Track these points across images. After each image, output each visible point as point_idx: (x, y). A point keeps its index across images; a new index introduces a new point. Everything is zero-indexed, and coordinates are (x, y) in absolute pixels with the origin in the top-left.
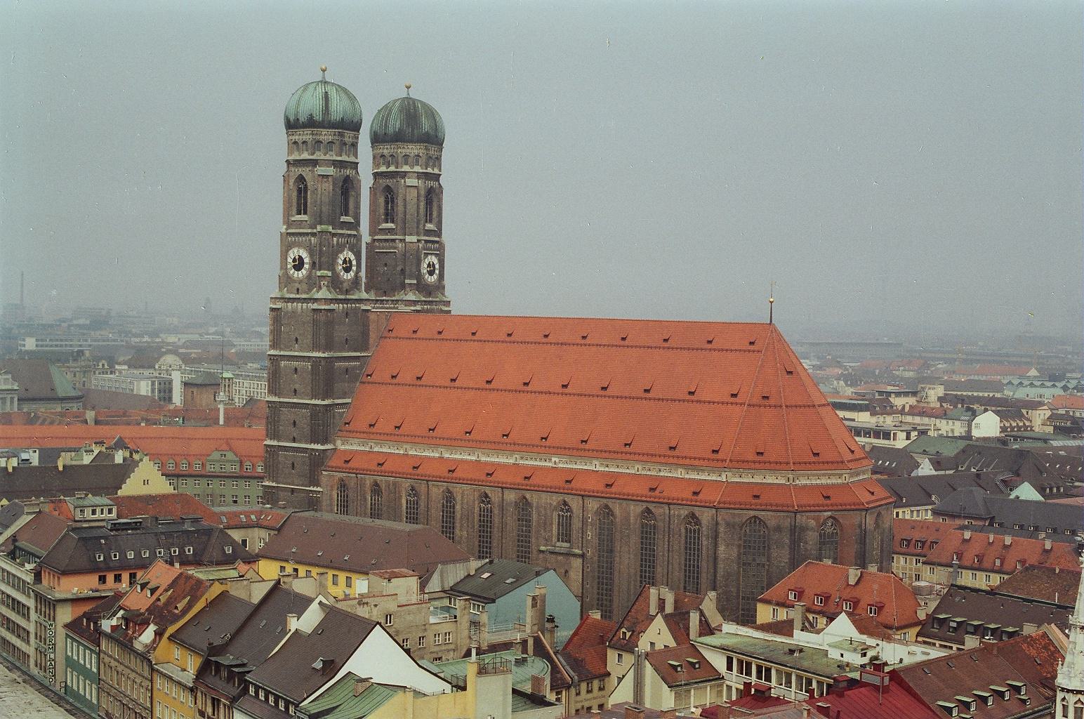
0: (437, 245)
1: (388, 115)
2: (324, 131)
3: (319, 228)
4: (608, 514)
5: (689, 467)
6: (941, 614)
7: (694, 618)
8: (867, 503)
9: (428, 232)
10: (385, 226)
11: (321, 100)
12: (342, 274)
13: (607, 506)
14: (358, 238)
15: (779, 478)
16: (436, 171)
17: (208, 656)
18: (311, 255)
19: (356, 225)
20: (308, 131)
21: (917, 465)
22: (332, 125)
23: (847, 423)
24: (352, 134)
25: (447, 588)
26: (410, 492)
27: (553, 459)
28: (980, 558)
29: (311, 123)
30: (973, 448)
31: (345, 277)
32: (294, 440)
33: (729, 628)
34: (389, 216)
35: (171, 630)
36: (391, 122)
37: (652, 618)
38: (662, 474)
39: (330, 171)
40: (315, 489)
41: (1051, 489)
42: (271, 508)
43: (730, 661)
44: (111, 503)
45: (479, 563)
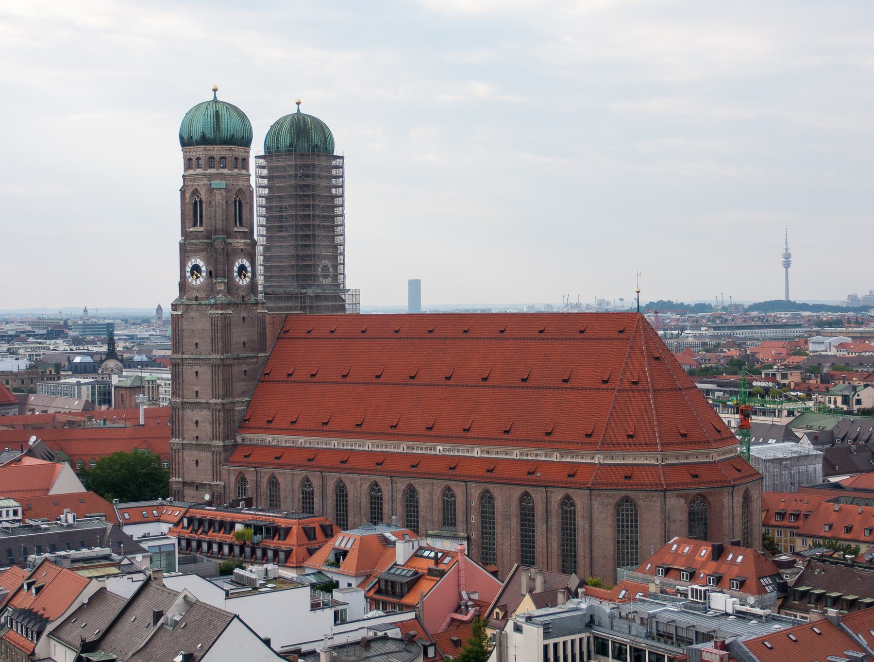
1: (279, 130)
2: (217, 147)
4: (490, 498)
5: (564, 451)
6: (802, 586)
8: (734, 480)
11: (212, 118)
12: (237, 280)
13: (487, 491)
14: (254, 244)
15: (648, 458)
17: (80, 653)
18: (207, 264)
20: (202, 147)
24: (242, 149)
26: (306, 483)
27: (438, 448)
29: (204, 140)
31: (241, 283)
35: (50, 628)
36: (282, 137)
38: (539, 458)
44: (16, 504)
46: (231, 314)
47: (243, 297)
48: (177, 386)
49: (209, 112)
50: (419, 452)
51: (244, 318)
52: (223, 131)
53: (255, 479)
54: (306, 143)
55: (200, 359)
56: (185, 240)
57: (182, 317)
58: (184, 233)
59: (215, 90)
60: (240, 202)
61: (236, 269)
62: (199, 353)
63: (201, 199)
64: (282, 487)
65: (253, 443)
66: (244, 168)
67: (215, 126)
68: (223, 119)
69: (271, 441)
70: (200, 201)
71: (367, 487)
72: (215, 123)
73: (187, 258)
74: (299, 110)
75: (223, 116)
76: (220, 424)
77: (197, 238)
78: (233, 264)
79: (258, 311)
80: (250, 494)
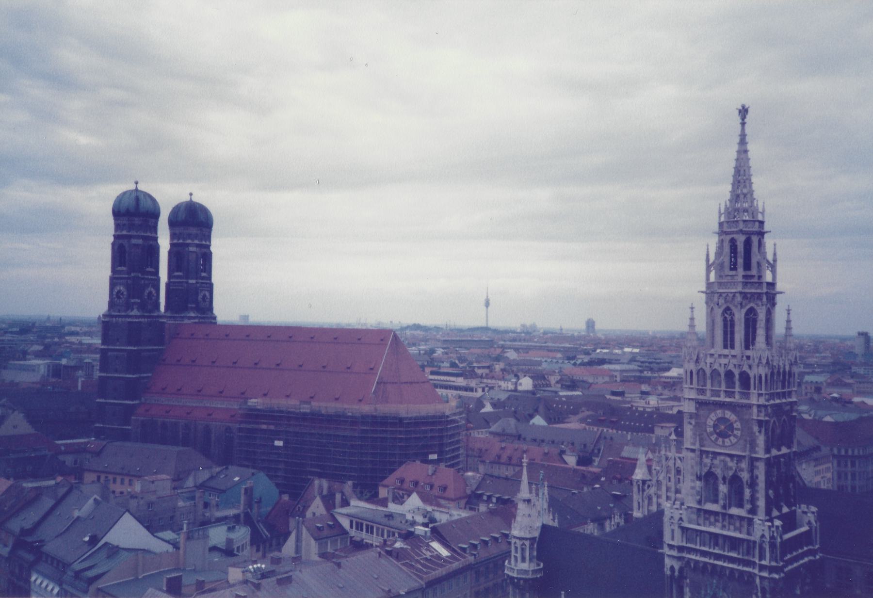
0: (208, 285)
2: (136, 219)
3: (133, 275)
7: (338, 496)
9: (203, 278)
10: (177, 274)
16: (208, 243)
19: (156, 272)
21: (483, 406)
23: (431, 382)
24: (153, 221)
25: (198, 484)
28: (510, 458)
30: (516, 396)
32: (115, 399)
33: (354, 502)
34: (179, 269)
37: (315, 497)
39: (140, 242)
40: (127, 427)
41: (555, 419)
42: (95, 440)
43: (351, 522)
45: (218, 469)
58: (114, 270)
59: (137, 183)
61: (146, 294)
74: (191, 199)
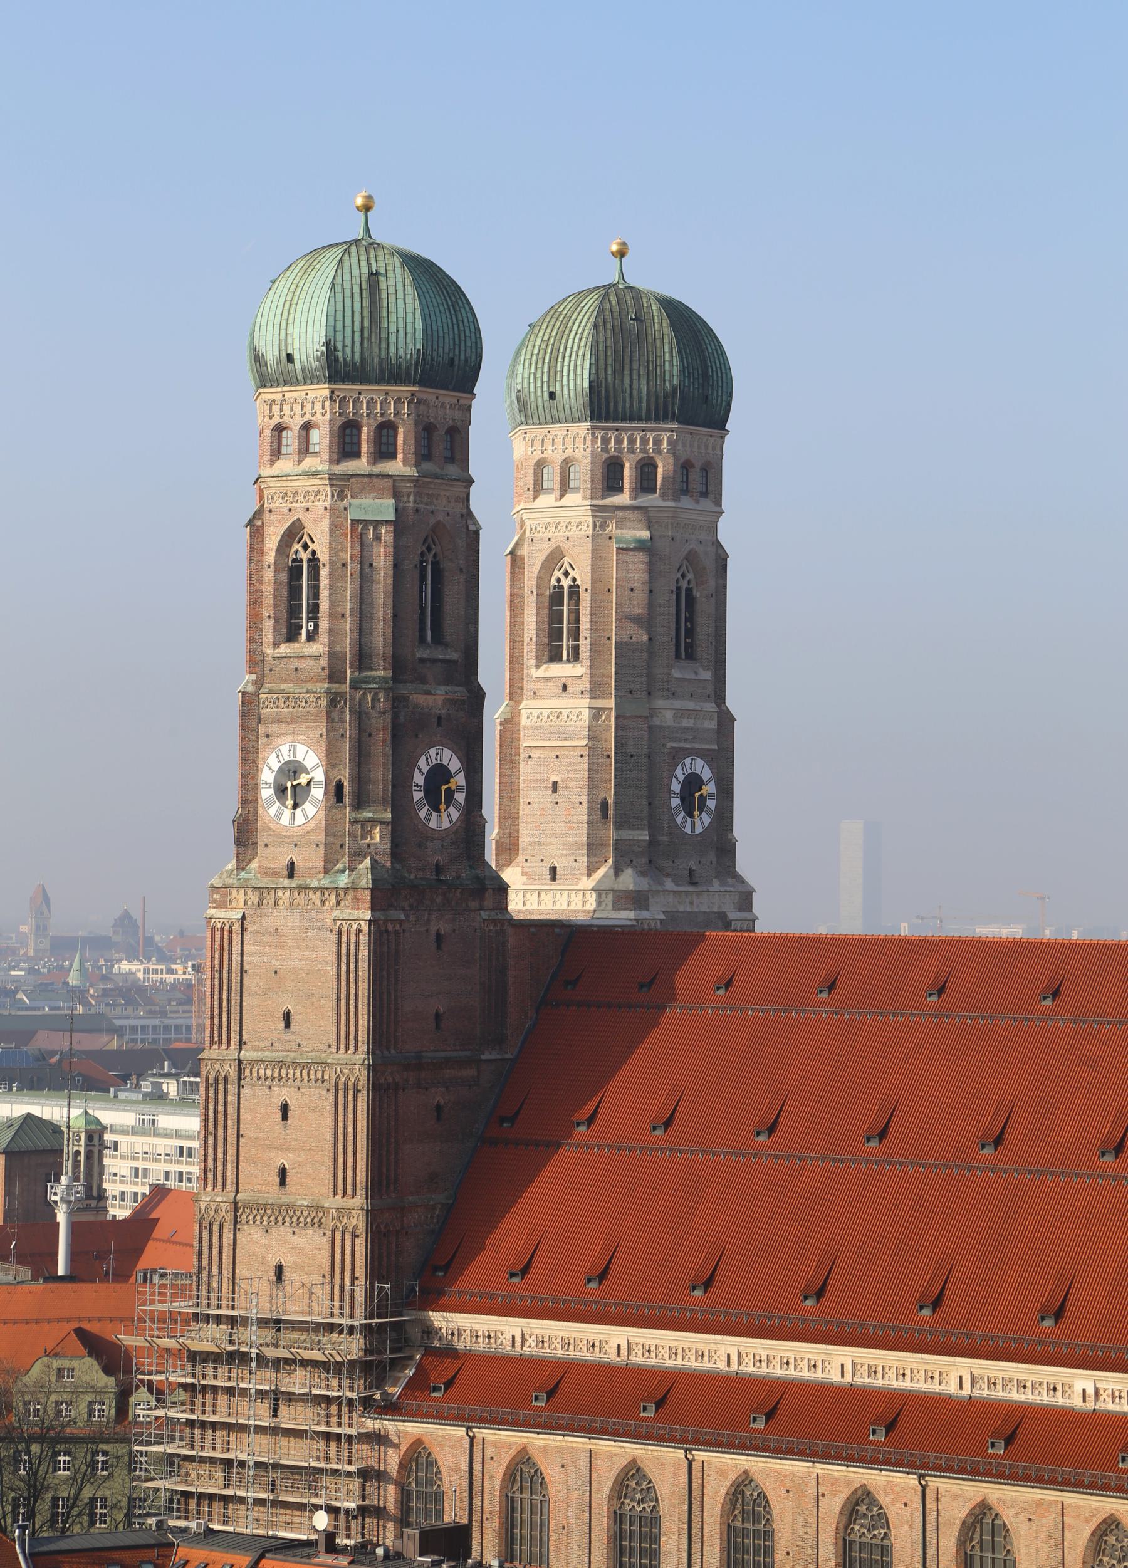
2: (372, 392)
11: (357, 297)
12: (422, 814)
18: (331, 761)
22: (391, 374)
24: (449, 397)
27: (1079, 1386)
31: (433, 824)
46: (401, 922)
47: (438, 868)
48: (220, 1151)
49: (347, 277)
50: (1015, 1396)
51: (439, 937)
52: (393, 339)
53: (465, 1466)
54: (644, 381)
55: (295, 1064)
56: (260, 683)
57: (243, 929)
58: (256, 662)
60: (435, 565)
61: (419, 779)
62: (294, 1046)
63: (314, 553)
64: (555, 1492)
65: (464, 1344)
66: (451, 459)
67: (366, 323)
68: (392, 299)
69: (518, 1339)
70: (309, 561)
71: (838, 1509)
72: (366, 313)
73: (262, 741)
75: (391, 290)
76: (354, 1279)
77: (297, 676)
78: (414, 765)
79: (484, 915)
80: (453, 1512)
